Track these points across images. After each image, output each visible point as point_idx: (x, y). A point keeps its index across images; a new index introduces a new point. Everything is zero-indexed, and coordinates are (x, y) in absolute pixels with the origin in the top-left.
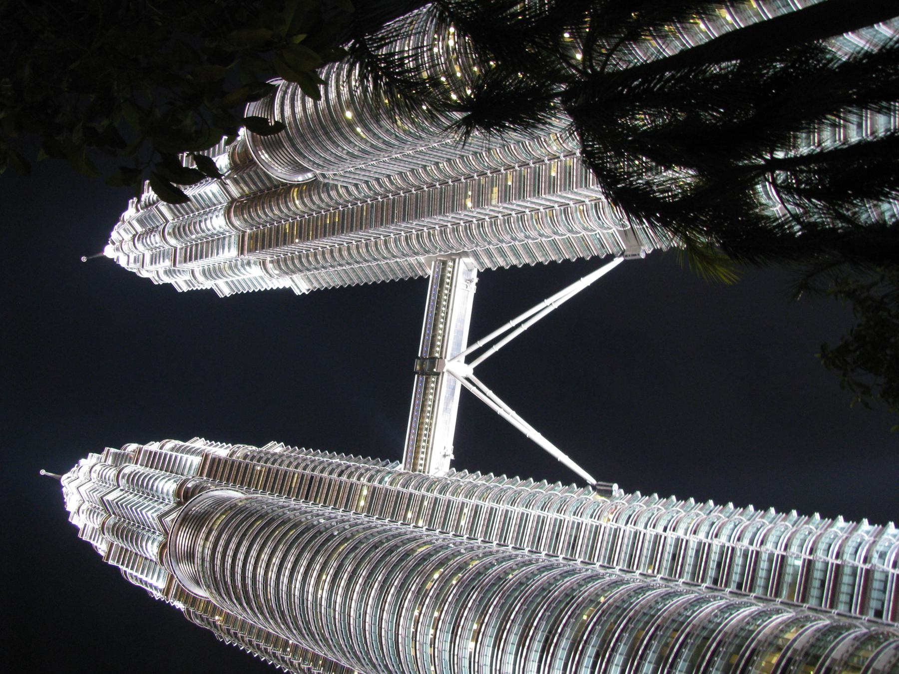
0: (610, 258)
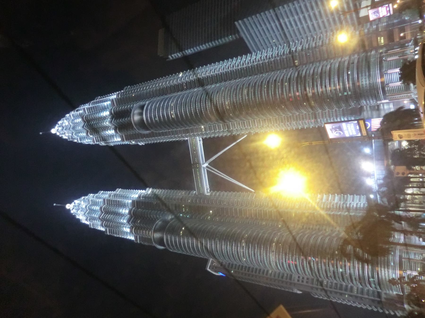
0: (243, 135)
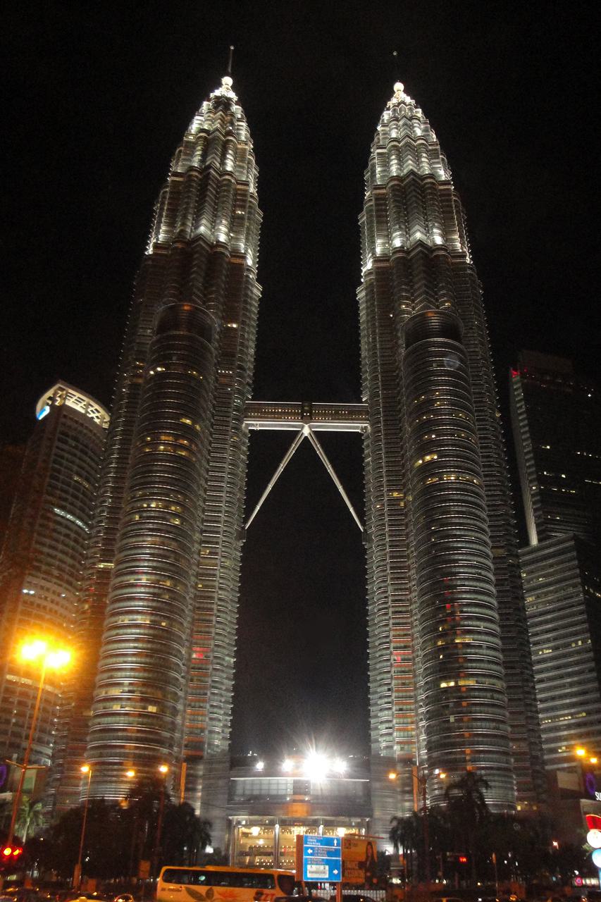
0: (363, 523)
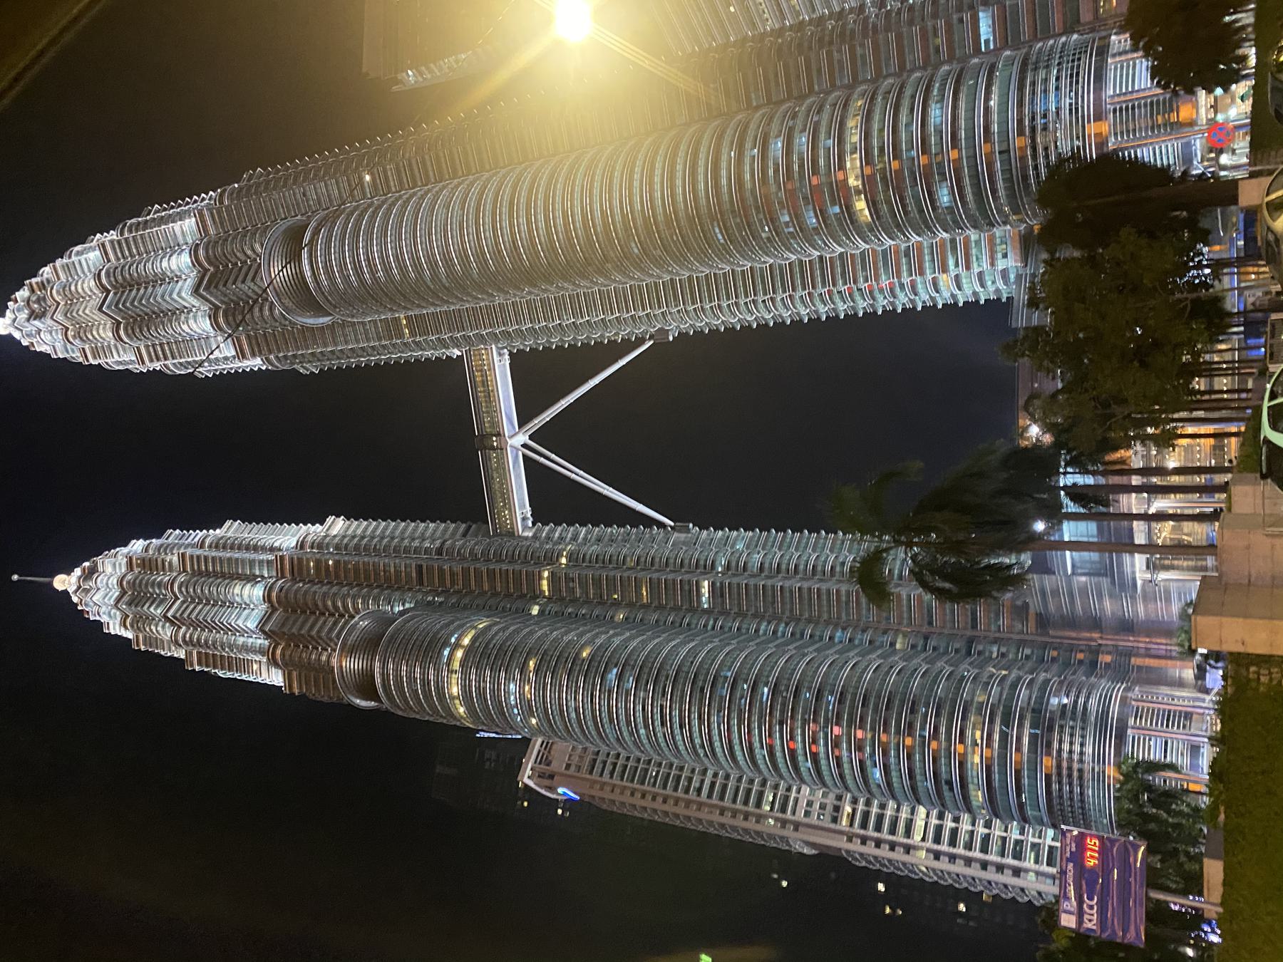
0: (640, 341)
